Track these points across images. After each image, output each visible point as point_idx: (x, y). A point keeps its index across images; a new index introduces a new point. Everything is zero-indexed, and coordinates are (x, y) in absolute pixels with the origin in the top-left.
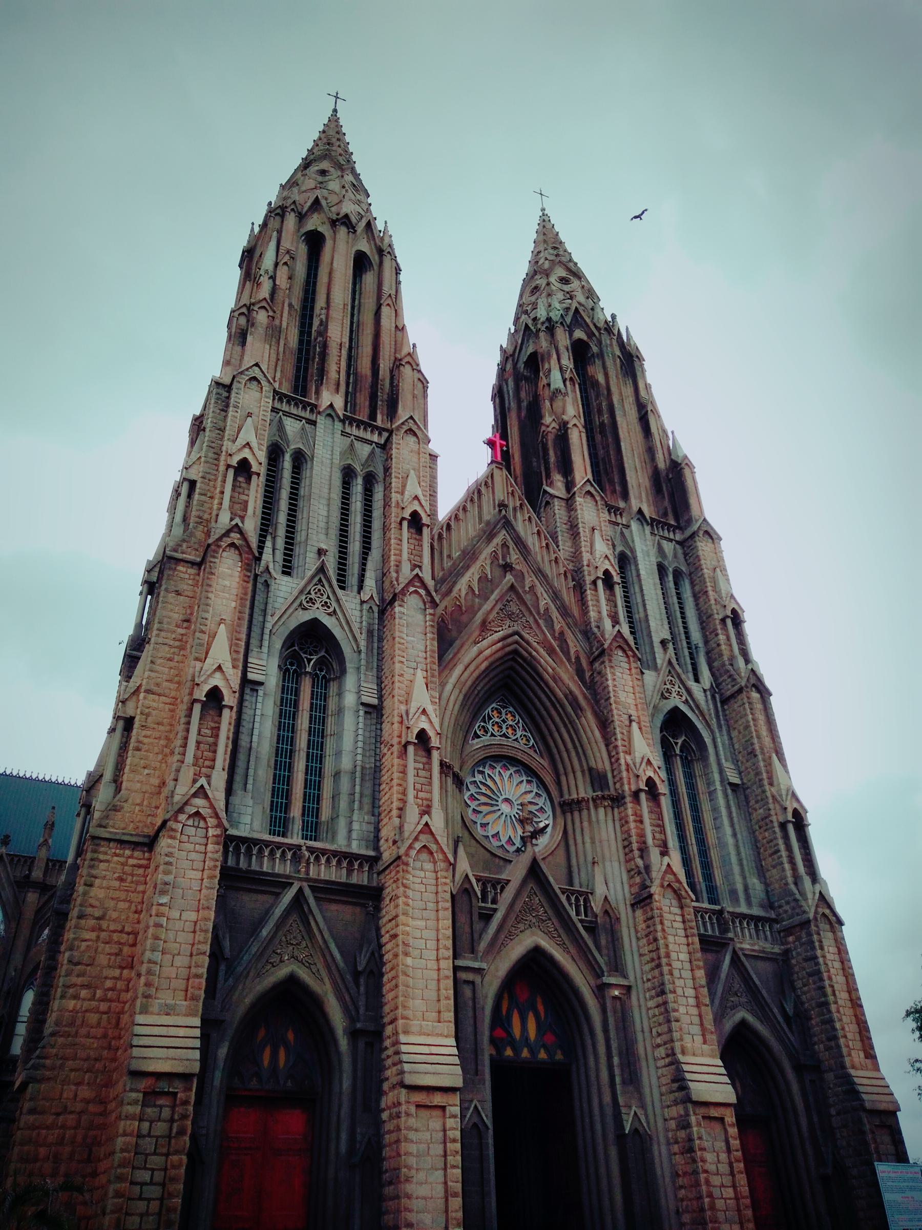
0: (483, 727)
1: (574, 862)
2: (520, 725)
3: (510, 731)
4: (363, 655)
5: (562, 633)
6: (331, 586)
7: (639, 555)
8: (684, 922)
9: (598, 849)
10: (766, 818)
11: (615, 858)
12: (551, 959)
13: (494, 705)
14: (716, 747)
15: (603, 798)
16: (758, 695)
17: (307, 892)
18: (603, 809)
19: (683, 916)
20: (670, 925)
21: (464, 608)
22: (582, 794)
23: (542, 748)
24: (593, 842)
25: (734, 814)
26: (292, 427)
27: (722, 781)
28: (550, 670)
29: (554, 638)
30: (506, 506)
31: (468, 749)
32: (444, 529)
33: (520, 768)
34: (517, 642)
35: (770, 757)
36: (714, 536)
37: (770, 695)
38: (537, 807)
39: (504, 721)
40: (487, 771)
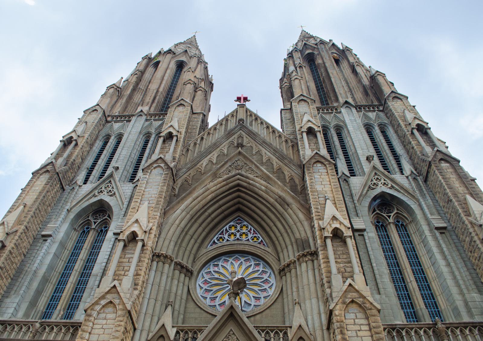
0: (221, 238)
1: (286, 310)
2: (252, 231)
3: (244, 236)
4: (124, 210)
5: (280, 169)
6: (115, 182)
7: (348, 121)
8: (370, 330)
9: (301, 294)
10: (471, 241)
11: (314, 295)
13: (232, 223)
14: (422, 209)
15: (304, 255)
16: (448, 165)
18: (305, 264)
19: (369, 325)
20: (354, 334)
21: (203, 172)
22: (292, 258)
23: (267, 241)
24: (298, 291)
25: (445, 249)
27: (431, 230)
28: (263, 188)
29: (273, 173)
31: (203, 251)
32: (199, 140)
33: (250, 257)
34: (239, 179)
35: (465, 199)
36: (402, 97)
37: (459, 161)
38: (263, 280)
39: (238, 231)
40: (220, 263)
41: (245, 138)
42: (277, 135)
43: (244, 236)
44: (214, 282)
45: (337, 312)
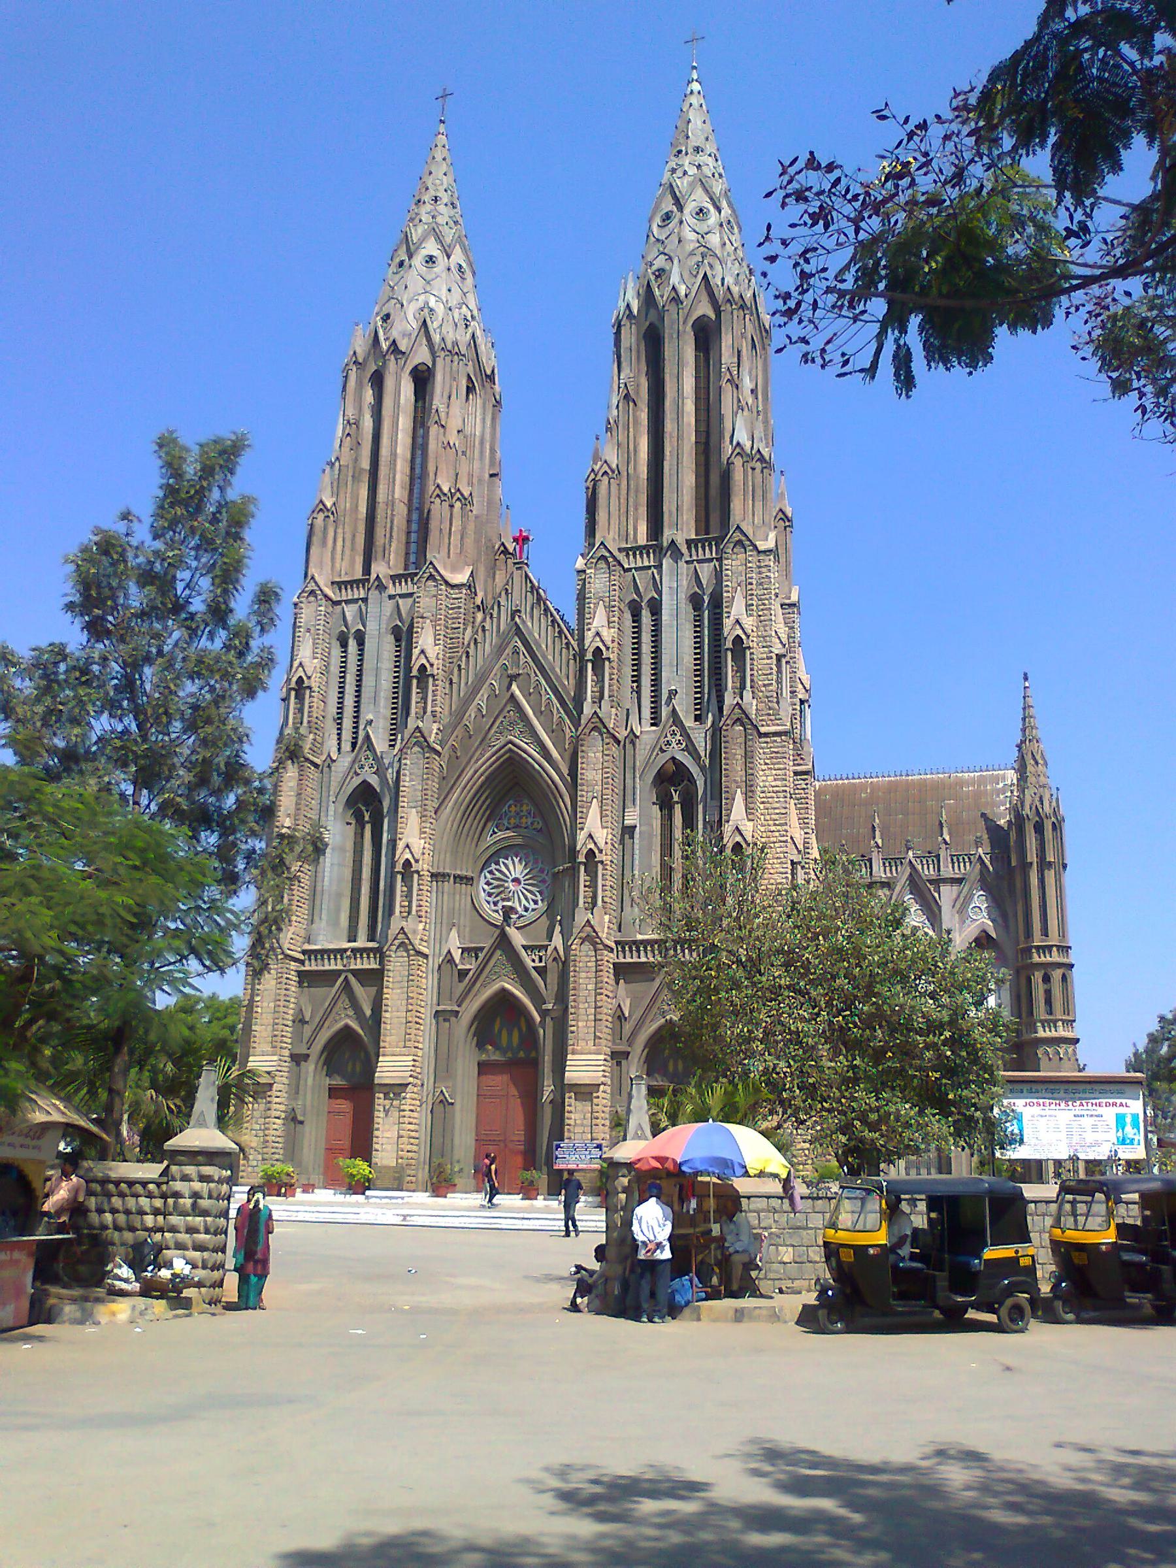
12: (512, 995)
13: (511, 802)
17: (350, 977)
26: (350, 611)
30: (519, 611)
32: (464, 658)
34: (510, 750)
41: (522, 656)
42: (564, 641)
43: (524, 820)
44: (496, 883)
45: (573, 947)
